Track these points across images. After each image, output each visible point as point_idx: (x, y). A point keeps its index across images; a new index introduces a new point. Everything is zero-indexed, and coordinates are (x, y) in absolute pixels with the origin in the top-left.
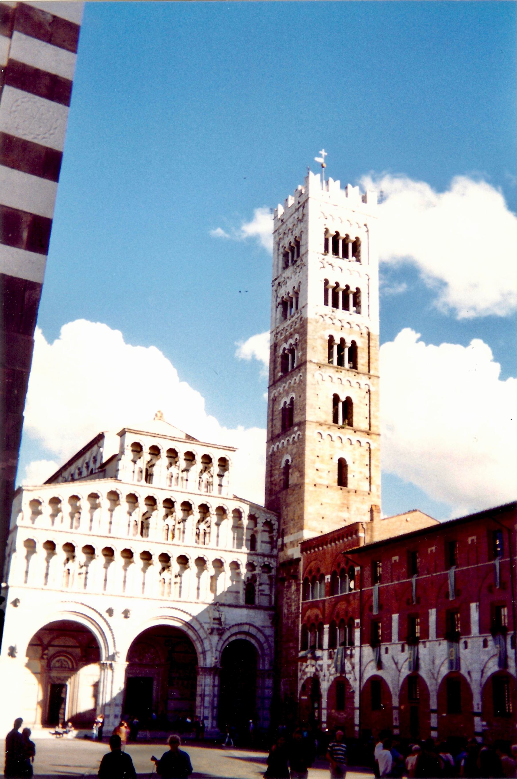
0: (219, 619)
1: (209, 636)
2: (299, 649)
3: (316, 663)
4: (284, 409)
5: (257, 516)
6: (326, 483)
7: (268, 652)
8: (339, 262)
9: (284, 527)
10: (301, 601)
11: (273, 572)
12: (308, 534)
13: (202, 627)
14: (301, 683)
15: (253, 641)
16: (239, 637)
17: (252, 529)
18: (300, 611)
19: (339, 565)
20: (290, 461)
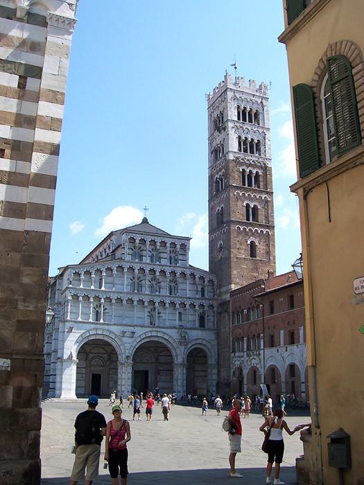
0: (185, 337)
4: (218, 214)
6: (243, 256)
8: (247, 125)
11: (215, 308)
12: (233, 287)
13: (175, 342)
14: (232, 371)
15: (204, 348)
16: (196, 346)
19: (251, 304)
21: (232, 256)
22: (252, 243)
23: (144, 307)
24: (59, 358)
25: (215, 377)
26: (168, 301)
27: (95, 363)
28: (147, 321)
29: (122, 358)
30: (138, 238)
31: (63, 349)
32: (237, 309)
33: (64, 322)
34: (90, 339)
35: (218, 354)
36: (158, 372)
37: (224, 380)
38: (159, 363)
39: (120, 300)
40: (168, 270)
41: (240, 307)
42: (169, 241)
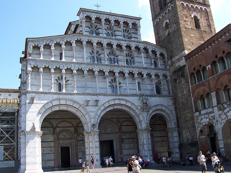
0: (146, 103)
1: (142, 112)
2: (194, 112)
3: (209, 116)
6: (190, 27)
7: (172, 118)
9: (171, 54)
10: (190, 86)
11: (169, 78)
12: (187, 52)
13: (138, 108)
15: (164, 114)
16: (157, 112)
17: (154, 58)
18: (191, 92)
19: (217, 56)
20: (168, 21)
21: (181, 26)
22: (195, 17)
23: (105, 78)
24: (22, 131)
25: (176, 139)
26: (126, 71)
27: (63, 137)
28: (109, 91)
29: (87, 127)
30: (94, 16)
32: (196, 69)
33: (25, 94)
35: (177, 118)
36: (122, 141)
37: (188, 141)
38: (122, 132)
39: (80, 71)
40: (124, 44)
41: (200, 66)
42: (122, 20)
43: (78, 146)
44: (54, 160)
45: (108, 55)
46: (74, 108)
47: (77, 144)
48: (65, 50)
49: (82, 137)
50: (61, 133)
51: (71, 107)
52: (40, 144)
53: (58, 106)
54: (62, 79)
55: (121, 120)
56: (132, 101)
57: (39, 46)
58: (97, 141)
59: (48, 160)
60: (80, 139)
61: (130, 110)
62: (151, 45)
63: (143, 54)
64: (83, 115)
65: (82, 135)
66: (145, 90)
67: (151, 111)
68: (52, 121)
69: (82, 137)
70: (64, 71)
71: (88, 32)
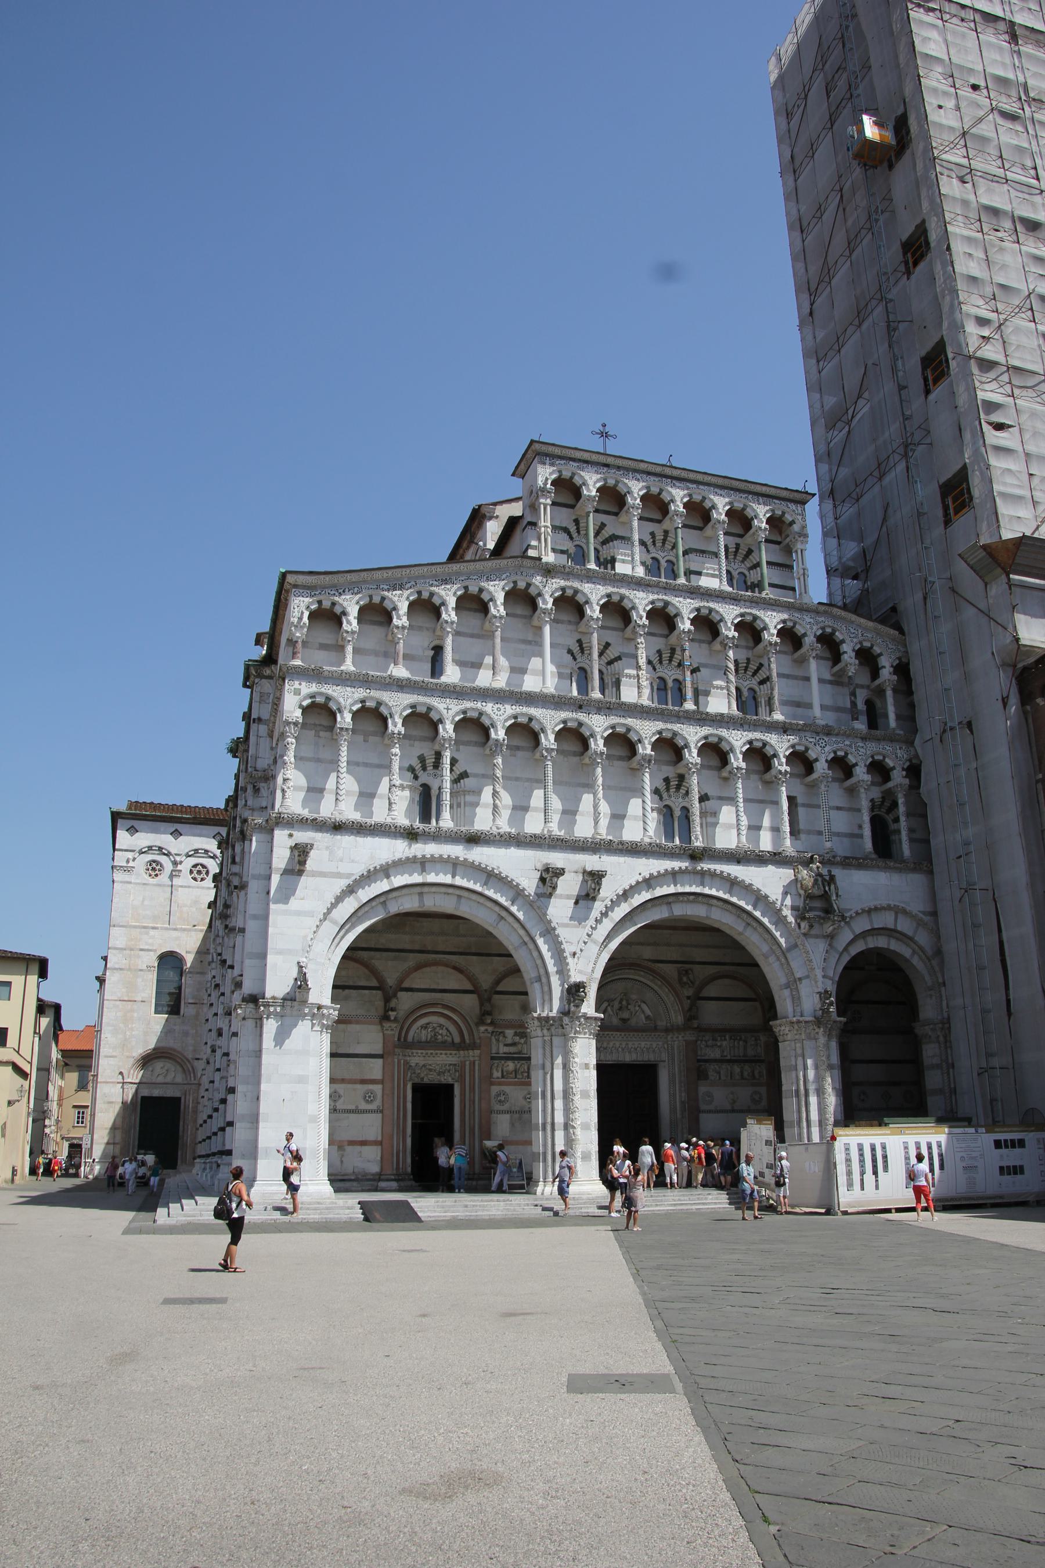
5: (877, 650)
16: (873, 943)
17: (868, 687)
23: (636, 772)
26: (738, 740)
27: (424, 1035)
31: (263, 956)
34: (394, 908)
38: (700, 1029)
40: (729, 614)
43: (492, 1084)
44: (379, 1143)
45: (649, 662)
46: (489, 904)
47: (491, 1074)
48: (457, 634)
49: (514, 1044)
50: (415, 1020)
51: (474, 897)
52: (326, 1062)
53: (418, 889)
54: (437, 764)
55: (701, 972)
56: (757, 884)
57: (338, 610)
58: (587, 1066)
59: (352, 1143)
60: (503, 1049)
61: (749, 924)
62: (852, 622)
63: (813, 665)
64: (527, 939)
65: (516, 1034)
66: (820, 833)
67: (846, 936)
68: (380, 962)
69: (514, 1044)
70: (447, 730)
71: (562, 552)
